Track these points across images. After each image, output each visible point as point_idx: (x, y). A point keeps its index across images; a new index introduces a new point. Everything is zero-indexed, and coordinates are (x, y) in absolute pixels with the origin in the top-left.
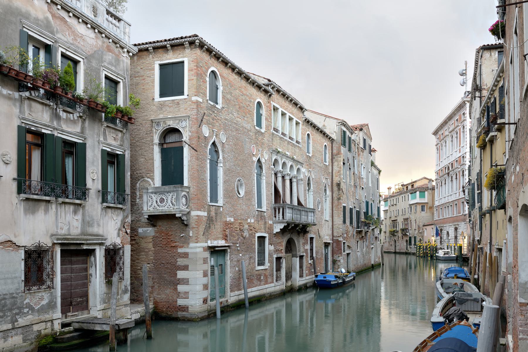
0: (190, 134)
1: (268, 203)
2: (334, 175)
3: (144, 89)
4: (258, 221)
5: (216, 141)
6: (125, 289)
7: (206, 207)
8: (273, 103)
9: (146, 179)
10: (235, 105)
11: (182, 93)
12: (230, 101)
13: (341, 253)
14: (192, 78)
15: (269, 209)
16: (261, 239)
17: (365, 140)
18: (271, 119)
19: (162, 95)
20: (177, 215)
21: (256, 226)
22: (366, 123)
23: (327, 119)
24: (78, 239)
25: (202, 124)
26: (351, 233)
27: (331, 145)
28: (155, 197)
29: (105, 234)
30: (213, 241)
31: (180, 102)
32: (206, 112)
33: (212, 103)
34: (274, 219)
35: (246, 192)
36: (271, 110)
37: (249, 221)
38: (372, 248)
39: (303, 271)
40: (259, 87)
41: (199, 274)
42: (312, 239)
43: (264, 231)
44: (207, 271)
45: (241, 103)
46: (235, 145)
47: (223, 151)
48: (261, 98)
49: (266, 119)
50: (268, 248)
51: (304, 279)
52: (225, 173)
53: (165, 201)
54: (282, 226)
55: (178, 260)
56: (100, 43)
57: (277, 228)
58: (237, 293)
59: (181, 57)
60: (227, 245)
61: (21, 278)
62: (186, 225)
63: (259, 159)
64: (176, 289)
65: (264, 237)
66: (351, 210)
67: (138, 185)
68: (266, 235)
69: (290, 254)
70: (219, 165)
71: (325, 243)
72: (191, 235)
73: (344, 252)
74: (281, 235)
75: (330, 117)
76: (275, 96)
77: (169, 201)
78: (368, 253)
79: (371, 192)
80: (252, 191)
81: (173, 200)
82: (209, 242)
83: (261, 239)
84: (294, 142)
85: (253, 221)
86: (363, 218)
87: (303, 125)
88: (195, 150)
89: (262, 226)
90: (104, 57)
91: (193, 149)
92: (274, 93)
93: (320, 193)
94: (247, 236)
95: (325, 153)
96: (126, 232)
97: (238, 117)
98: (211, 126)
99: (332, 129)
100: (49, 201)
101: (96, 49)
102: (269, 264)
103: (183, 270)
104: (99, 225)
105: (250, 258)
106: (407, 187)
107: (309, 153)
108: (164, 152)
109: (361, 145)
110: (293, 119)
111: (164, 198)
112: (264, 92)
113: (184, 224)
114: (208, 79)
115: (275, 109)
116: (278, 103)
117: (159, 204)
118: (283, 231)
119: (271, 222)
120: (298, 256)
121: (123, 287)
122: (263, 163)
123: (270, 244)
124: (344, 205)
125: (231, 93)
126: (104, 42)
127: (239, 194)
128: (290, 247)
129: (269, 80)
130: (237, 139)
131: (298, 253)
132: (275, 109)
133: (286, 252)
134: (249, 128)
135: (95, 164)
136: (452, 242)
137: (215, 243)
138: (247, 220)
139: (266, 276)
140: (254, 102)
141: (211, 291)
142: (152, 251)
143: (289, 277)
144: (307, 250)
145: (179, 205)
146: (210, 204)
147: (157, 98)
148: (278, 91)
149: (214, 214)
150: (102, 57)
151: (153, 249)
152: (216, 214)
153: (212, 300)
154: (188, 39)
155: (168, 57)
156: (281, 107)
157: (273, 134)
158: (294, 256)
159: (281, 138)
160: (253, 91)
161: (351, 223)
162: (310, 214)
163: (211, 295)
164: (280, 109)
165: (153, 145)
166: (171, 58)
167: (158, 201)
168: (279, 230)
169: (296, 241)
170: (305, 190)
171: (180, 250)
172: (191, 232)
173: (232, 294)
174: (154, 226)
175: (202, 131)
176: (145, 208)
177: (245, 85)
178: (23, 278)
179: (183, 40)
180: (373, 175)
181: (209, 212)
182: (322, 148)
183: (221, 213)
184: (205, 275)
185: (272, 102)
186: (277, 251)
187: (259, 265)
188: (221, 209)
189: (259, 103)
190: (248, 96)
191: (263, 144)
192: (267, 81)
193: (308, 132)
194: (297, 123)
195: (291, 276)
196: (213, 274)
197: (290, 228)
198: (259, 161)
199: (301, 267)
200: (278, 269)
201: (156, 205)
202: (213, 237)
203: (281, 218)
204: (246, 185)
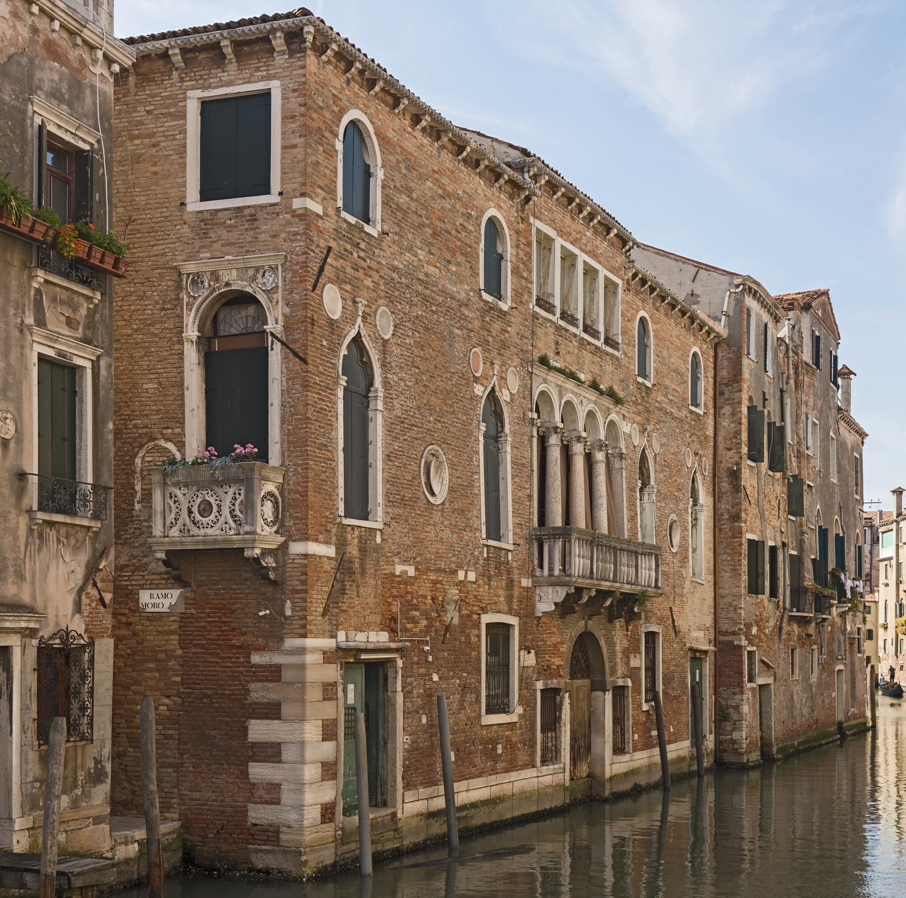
0: (287, 310)
2: (721, 446)
3: (156, 173)
4: (490, 578)
5: (363, 333)
6: (96, 768)
7: (334, 530)
9: (162, 443)
10: (421, 226)
11: (266, 190)
12: (405, 213)
13: (740, 684)
14: (294, 142)
15: (521, 542)
17: (816, 341)
18: (531, 272)
19: (204, 197)
20: (248, 553)
21: (483, 591)
22: (823, 287)
23: (702, 273)
25: (322, 280)
26: (772, 623)
27: (712, 353)
29: (39, 604)
30: (352, 633)
32: (333, 244)
33: (352, 220)
35: (451, 490)
36: (529, 244)
37: (461, 575)
38: (840, 671)
39: (623, 735)
41: (312, 731)
43: (505, 607)
44: (335, 721)
45: (439, 219)
46: (422, 348)
47: (383, 366)
48: (499, 207)
49: (516, 271)
51: (627, 757)
52: (389, 430)
53: (215, 508)
54: (560, 594)
55: (253, 686)
56: (24, 32)
57: (547, 601)
59: (263, 79)
60: (393, 645)
62: (274, 583)
63: (493, 389)
65: (507, 627)
66: (773, 550)
67: (138, 461)
68: (513, 621)
70: (371, 406)
71: (693, 650)
72: (288, 613)
73: (751, 679)
74: (557, 622)
77: (226, 511)
78: (826, 686)
79: (837, 499)
80: (471, 485)
81: (237, 508)
82: (341, 636)
83: (499, 632)
84: (600, 343)
85: (472, 576)
86: (809, 579)
87: (627, 290)
89: (501, 592)
90: (38, 74)
91: (296, 355)
92: (538, 192)
94: (456, 621)
96: (102, 600)
97: (429, 263)
98: (348, 287)
101: (12, 50)
102: (519, 710)
104: (20, 576)
107: (645, 377)
109: (807, 356)
110: (596, 271)
111: (212, 500)
112: (508, 188)
114: (339, 146)
116: (552, 223)
117: (198, 517)
118: (565, 608)
119: (526, 582)
120: (608, 687)
121: (91, 764)
122: (503, 404)
123: (525, 647)
125: (409, 191)
126: (35, 30)
127: (433, 494)
128: (586, 660)
129: (525, 152)
130: (427, 329)
131: (609, 679)
132: (545, 243)
133: (573, 676)
134: (462, 296)
135: (11, 394)
137: (360, 639)
138: (454, 572)
139: (511, 747)
140: (479, 218)
141: (346, 784)
142: (176, 658)
143: (582, 748)
145: (253, 524)
147: (194, 204)
148: (553, 185)
149: (355, 552)
150: (31, 76)
151: (179, 652)
152: (363, 550)
153: (347, 811)
154: (282, 22)
155: (225, 77)
156: (561, 233)
157: (535, 316)
159: (559, 328)
163: (344, 794)
164: (559, 242)
166: (235, 84)
167: (195, 509)
169: (603, 643)
171: (256, 659)
172: (288, 604)
173: (410, 795)
174: (179, 581)
175: (321, 304)
177: (449, 165)
179: (268, 26)
180: (842, 445)
181: (341, 545)
182: (686, 361)
183: (378, 548)
184: (329, 733)
185: (532, 219)
186: (544, 671)
187: (489, 711)
188: (379, 540)
189: (492, 221)
190: (459, 199)
191: (504, 345)
193: (642, 313)
194: (610, 286)
195: (589, 749)
196: (351, 733)
197: (585, 599)
198: (492, 397)
199: (619, 721)
200: (551, 724)
201: (188, 520)
202: (354, 621)
203: (557, 568)
204: (453, 466)
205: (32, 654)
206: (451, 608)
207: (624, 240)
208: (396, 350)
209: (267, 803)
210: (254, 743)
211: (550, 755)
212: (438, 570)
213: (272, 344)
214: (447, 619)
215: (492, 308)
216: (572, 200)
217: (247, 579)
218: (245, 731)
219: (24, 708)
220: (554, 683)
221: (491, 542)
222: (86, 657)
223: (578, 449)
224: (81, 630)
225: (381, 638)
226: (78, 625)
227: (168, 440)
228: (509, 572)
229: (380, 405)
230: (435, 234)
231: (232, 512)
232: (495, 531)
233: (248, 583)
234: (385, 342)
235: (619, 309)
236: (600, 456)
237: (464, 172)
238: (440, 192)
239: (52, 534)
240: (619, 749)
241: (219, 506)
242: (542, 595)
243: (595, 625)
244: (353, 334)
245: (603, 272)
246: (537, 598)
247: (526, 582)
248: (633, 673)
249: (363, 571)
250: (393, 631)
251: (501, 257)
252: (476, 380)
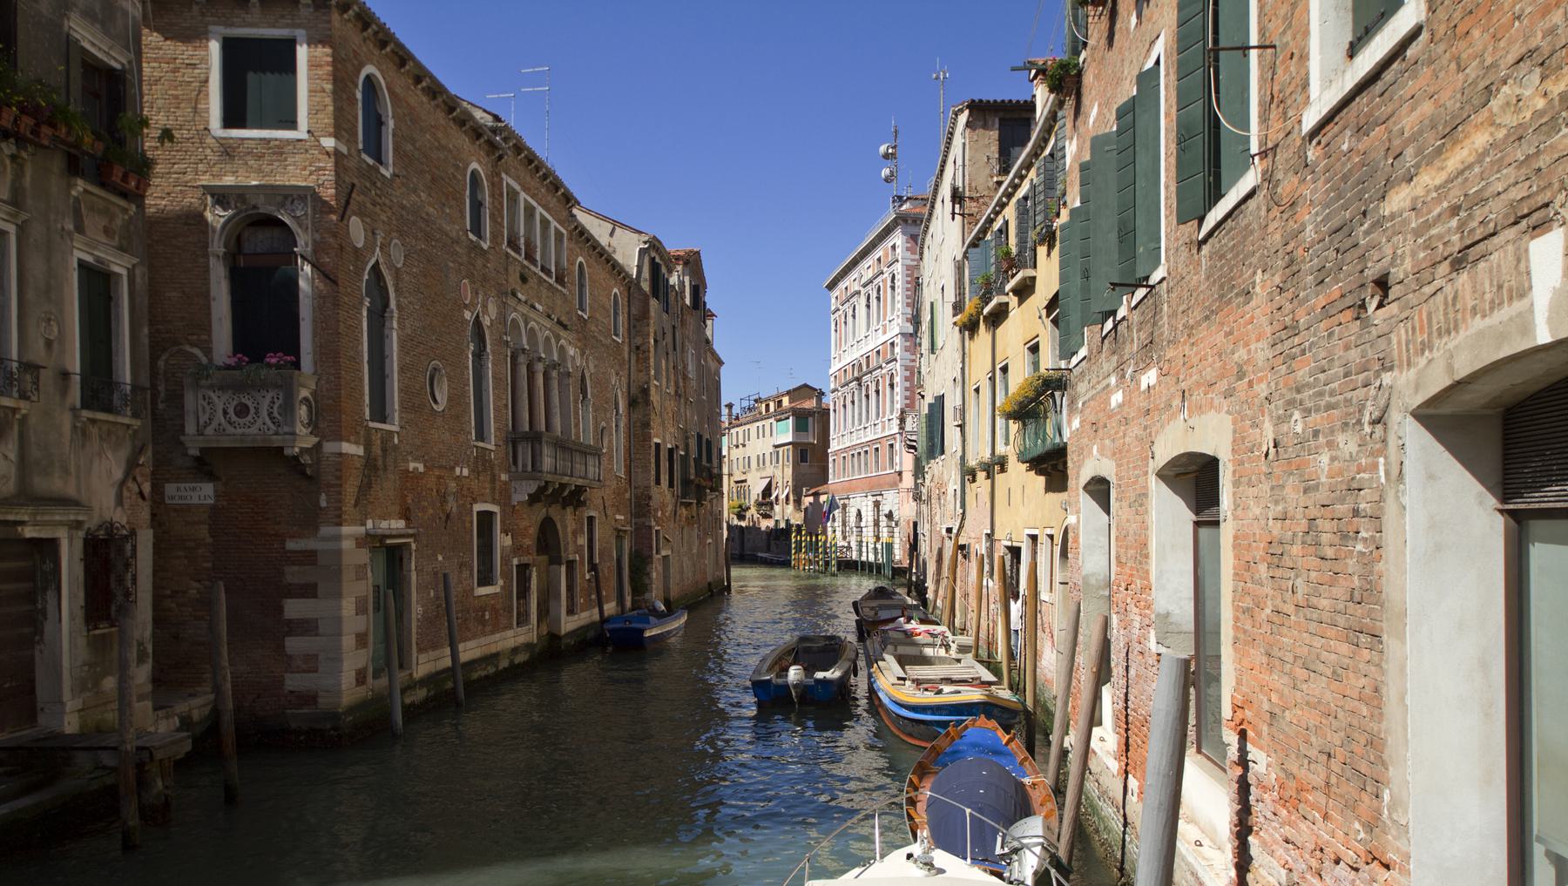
1: (497, 429)
8: (507, 180)
9: (188, 348)
20: (288, 452)
21: (474, 484)
28: (220, 401)
35: (450, 399)
36: (501, 195)
37: (458, 470)
40: (477, 132)
42: (591, 519)
48: (480, 162)
49: (492, 216)
50: (502, 541)
53: (252, 411)
54: (532, 487)
58: (432, 654)
59: (287, 26)
62: (310, 478)
65: (491, 514)
66: (671, 451)
69: (544, 558)
72: (323, 504)
76: (509, 158)
77: (265, 413)
80: (464, 394)
85: (466, 472)
87: (570, 239)
93: (605, 410)
95: (616, 314)
97: (430, 204)
99: (628, 251)
105: (461, 565)
106: (780, 402)
108: (238, 277)
111: (249, 403)
113: (304, 474)
116: (517, 179)
117: (234, 418)
118: (534, 499)
119: (504, 477)
123: (505, 531)
125: (413, 141)
127: (435, 401)
128: (548, 540)
129: (497, 118)
136: (868, 533)
138: (453, 469)
139: (494, 611)
140: (466, 168)
145: (293, 424)
146: (372, 424)
148: (519, 148)
149: (379, 452)
155: (248, 18)
156: (526, 189)
158: (556, 560)
160: (461, 140)
161: (671, 485)
162: (591, 461)
164: (523, 195)
165: (206, 256)
167: (231, 411)
170: (576, 402)
172: (323, 496)
174: (211, 476)
176: (190, 428)
181: (368, 446)
183: (396, 448)
186: (517, 549)
190: (450, 151)
191: (485, 279)
192: (490, 118)
193: (580, 259)
194: (559, 235)
199: (570, 588)
200: (523, 592)
205: (79, 545)
206: (450, 499)
207: (569, 200)
209: (304, 671)
211: (523, 619)
212: (440, 467)
214: (448, 509)
215: (475, 247)
216: (532, 161)
218: (280, 609)
219: (72, 596)
220: (525, 560)
221: (481, 444)
222: (129, 547)
223: (540, 367)
224: (124, 522)
225: (398, 524)
226: (120, 517)
227: (192, 345)
228: (492, 468)
229: (395, 325)
230: (433, 180)
231: (270, 414)
232: (481, 436)
234: (397, 270)
235: (565, 254)
236: (554, 374)
237: (454, 130)
239: (94, 430)
240: (570, 612)
243: (554, 511)
244: (372, 262)
245: (554, 223)
247: (504, 477)
248: (579, 550)
249: (385, 469)
250: (407, 519)
251: (480, 204)
252: (466, 306)
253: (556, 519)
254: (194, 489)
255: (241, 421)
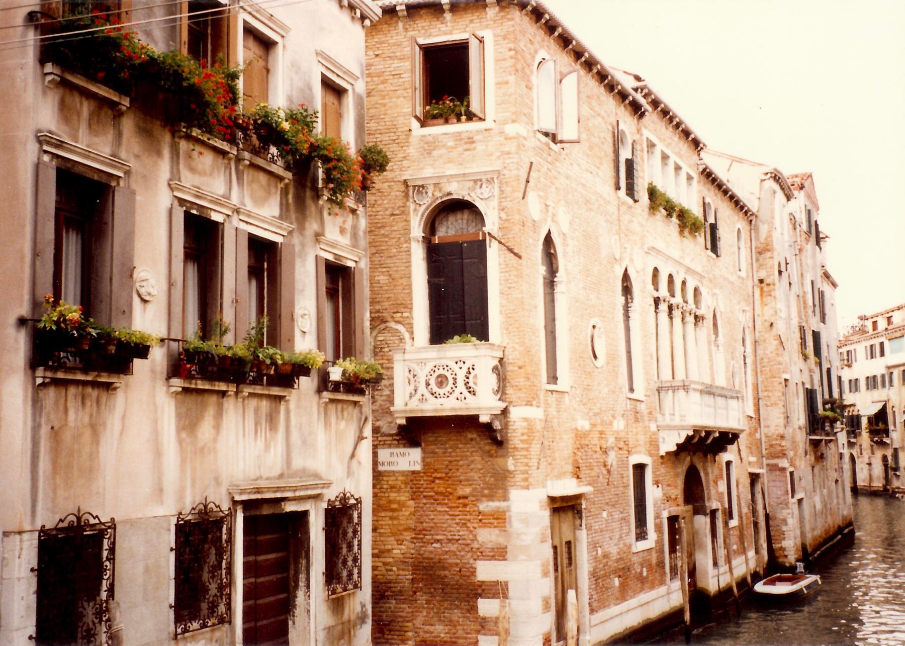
15: (649, 393)
16: (640, 469)
24: (278, 489)
31: (476, 138)
34: (659, 417)
50: (653, 494)
61: (168, 599)
64: (474, 609)
69: (690, 507)
75: (740, 161)
83: (640, 469)
87: (699, 182)
88: (516, 254)
100: (223, 394)
103: (493, 558)
115: (651, 145)
118: (681, 448)
124: (787, 376)
129: (638, 78)
131: (707, 504)
132: (651, 145)
138: (611, 424)
144: (722, 493)
148: (655, 103)
156: (662, 140)
168: (674, 448)
169: (702, 474)
170: (709, 343)
178: (172, 600)
192: (632, 78)
208: (570, 242)
210: (483, 582)
213: (490, 241)
217: (472, 440)
233: (473, 442)
238: (592, 112)
241: (455, 379)
242: (665, 436)
246: (661, 440)
253: (699, 466)
254: (404, 455)
255: (441, 391)
